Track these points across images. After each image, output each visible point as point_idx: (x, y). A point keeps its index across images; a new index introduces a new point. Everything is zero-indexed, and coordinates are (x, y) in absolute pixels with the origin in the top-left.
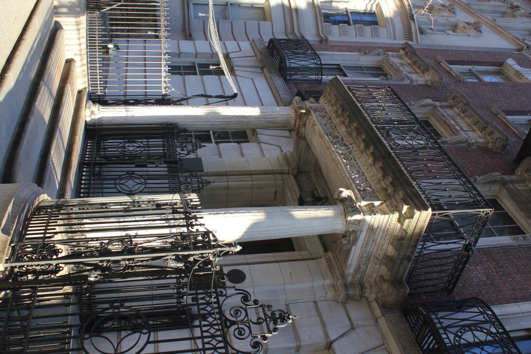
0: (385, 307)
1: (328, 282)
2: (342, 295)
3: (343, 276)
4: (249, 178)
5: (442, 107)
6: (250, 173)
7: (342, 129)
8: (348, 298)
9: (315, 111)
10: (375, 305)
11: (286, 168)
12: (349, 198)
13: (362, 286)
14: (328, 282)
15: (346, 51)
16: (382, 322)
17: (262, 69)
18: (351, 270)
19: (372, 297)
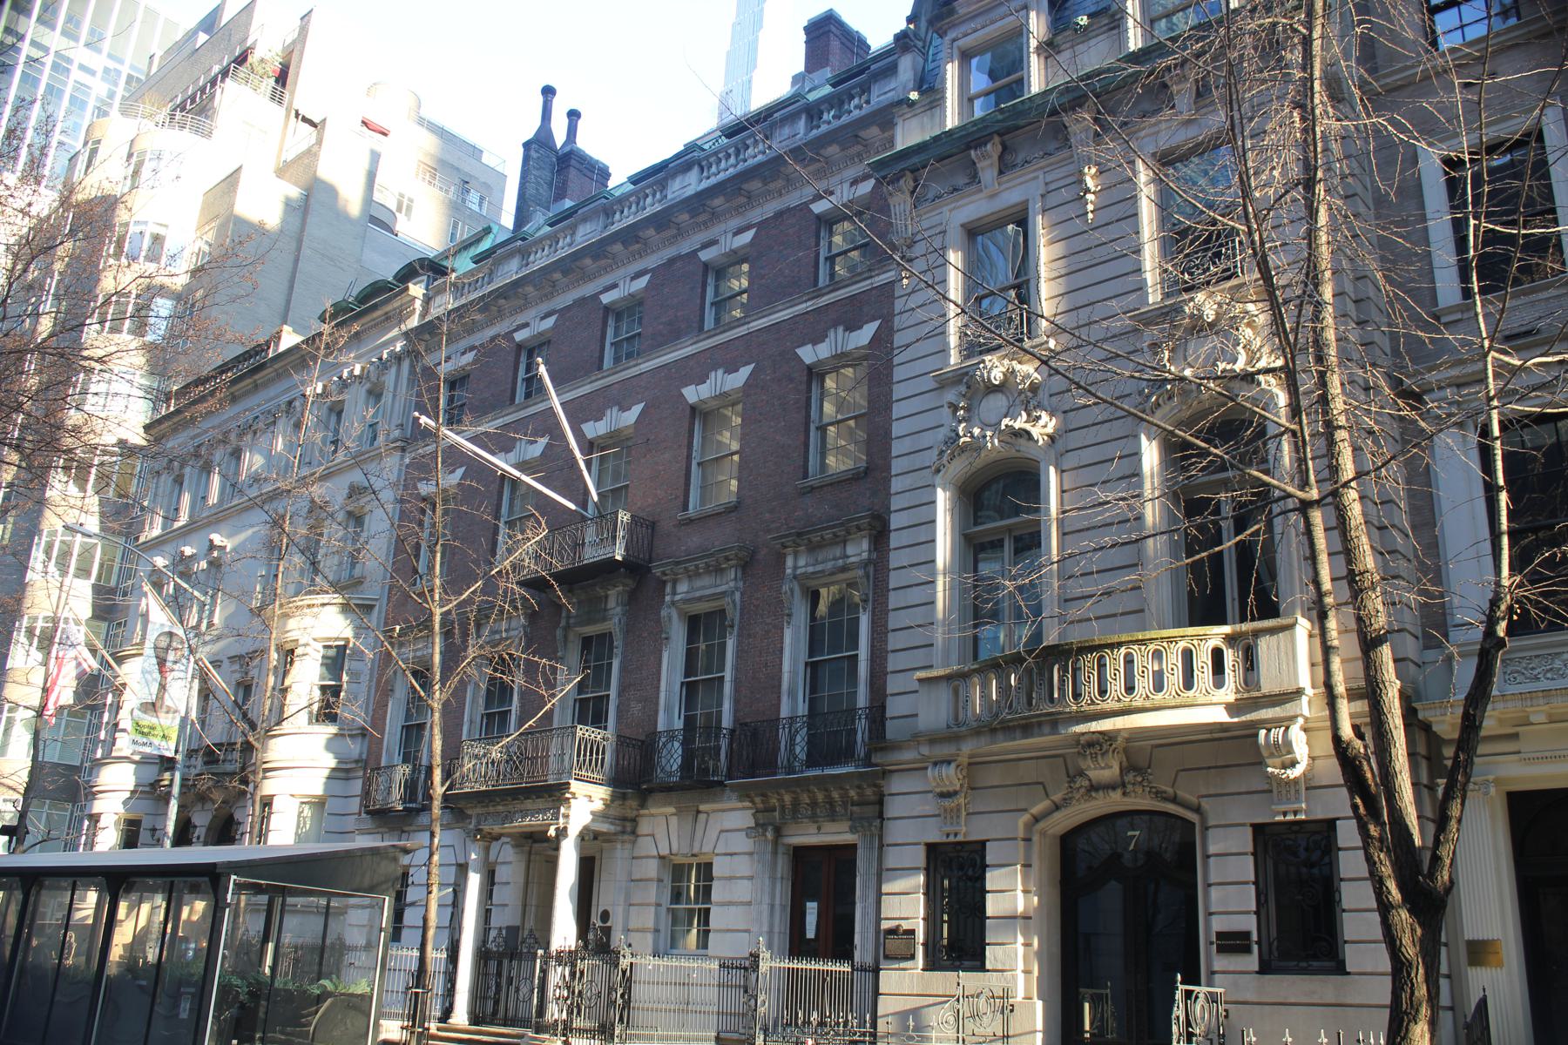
0: (643, 805)
1: (619, 846)
2: (632, 838)
3: (615, 834)
4: (530, 885)
6: (527, 883)
7: (500, 808)
8: (634, 832)
10: (642, 812)
11: (527, 849)
12: (557, 829)
13: (624, 819)
14: (619, 846)
15: (386, 712)
16: (653, 811)
17: (403, 832)
18: (612, 828)
19: (635, 813)
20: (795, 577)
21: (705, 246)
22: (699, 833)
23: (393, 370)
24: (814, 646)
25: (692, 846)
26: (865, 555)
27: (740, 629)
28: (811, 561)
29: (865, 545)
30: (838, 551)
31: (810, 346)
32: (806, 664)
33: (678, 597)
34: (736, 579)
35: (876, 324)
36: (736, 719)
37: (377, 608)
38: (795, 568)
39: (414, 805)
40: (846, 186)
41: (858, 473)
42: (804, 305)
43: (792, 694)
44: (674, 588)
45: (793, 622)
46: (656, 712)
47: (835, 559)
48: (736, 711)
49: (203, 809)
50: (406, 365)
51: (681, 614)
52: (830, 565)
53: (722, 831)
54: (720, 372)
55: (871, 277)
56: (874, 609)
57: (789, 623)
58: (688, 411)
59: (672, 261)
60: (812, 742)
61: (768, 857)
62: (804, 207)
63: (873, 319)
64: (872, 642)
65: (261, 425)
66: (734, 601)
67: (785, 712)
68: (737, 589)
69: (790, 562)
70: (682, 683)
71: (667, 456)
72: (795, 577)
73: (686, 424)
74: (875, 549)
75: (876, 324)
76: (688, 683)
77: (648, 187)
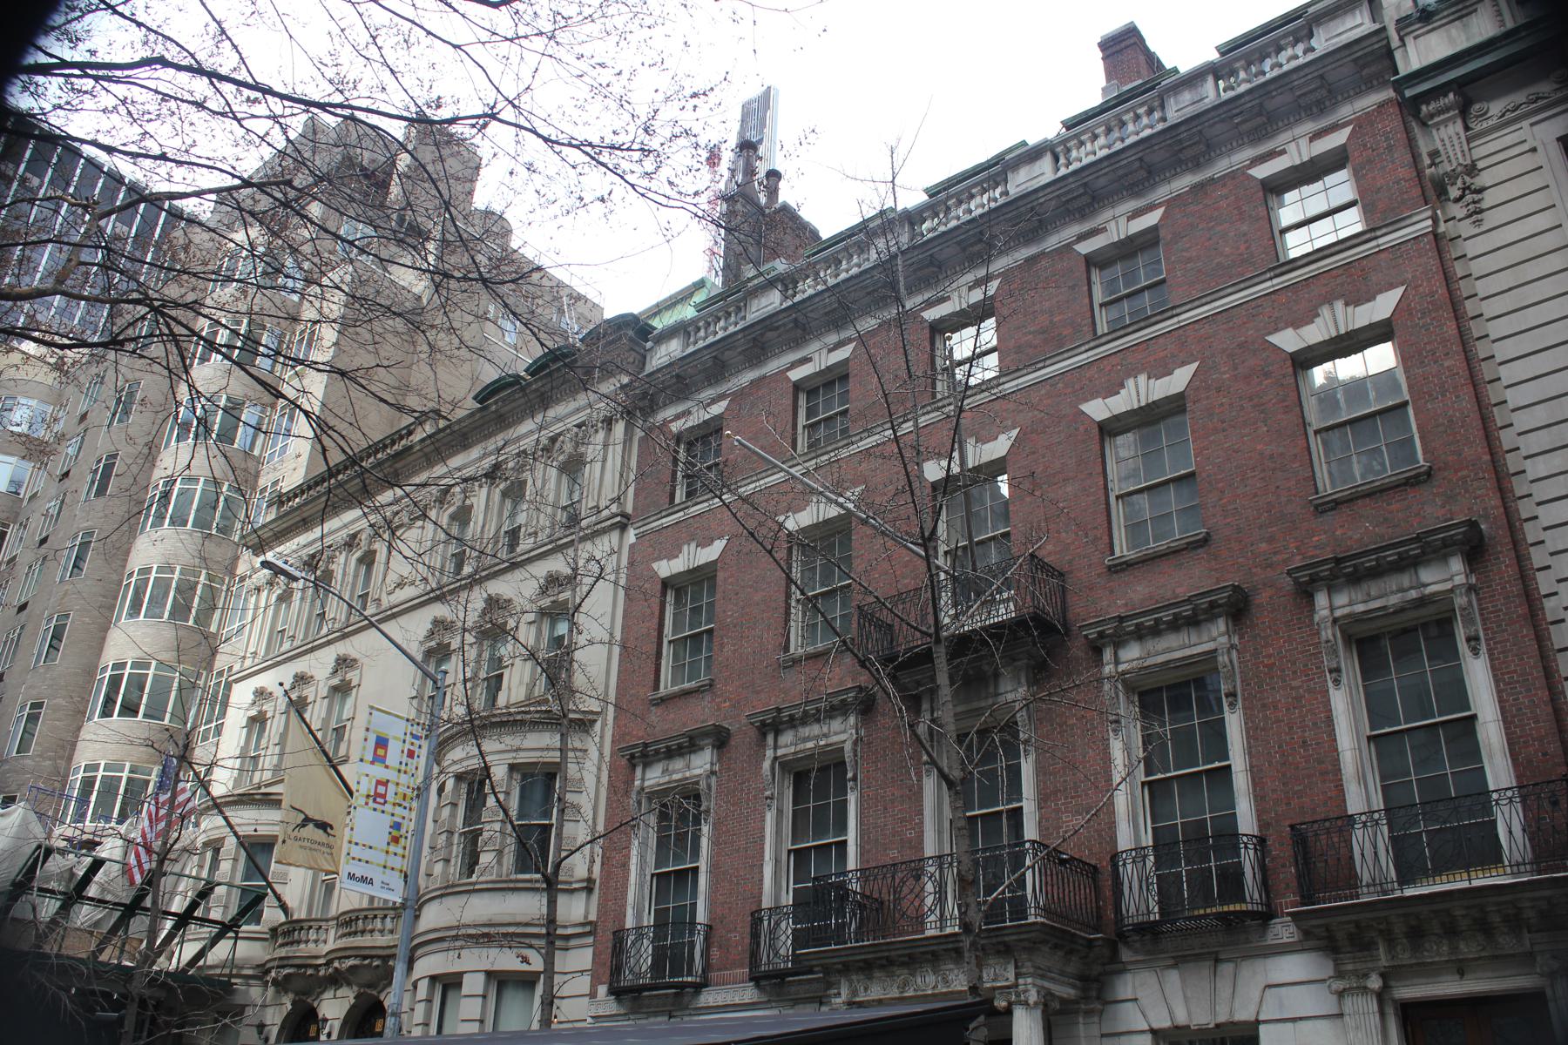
1: (1081, 1020)
3: (1076, 1002)
5: (776, 747)
9: (854, 993)
10: (1108, 968)
14: (1081, 1020)
20: (1335, 621)
21: (1082, 237)
22: (1224, 990)
23: (601, 435)
24: (1375, 717)
25: (1214, 1013)
26: (1460, 579)
27: (1244, 700)
28: (1360, 598)
29: (1457, 565)
30: (1405, 579)
31: (1290, 332)
32: (1369, 738)
33: (1121, 668)
34: (1227, 632)
35: (1399, 291)
36: (1263, 824)
37: (598, 726)
38: (1332, 609)
39: (690, 979)
40: (1303, 142)
41: (1417, 476)
42: (1269, 284)
43: (1362, 779)
44: (1116, 654)
45: (1344, 679)
46: (1112, 825)
47: (1402, 590)
48: (1260, 813)
49: (335, 997)
50: (619, 429)
51: (1130, 687)
52: (1394, 600)
53: (1270, 986)
54: (1142, 378)
55: (1376, 238)
56: (1490, 651)
57: (1337, 682)
58: (1096, 431)
59: (1031, 260)
60: (1399, 844)
61: (1375, 1019)
62: (1238, 176)
63: (1391, 287)
64: (1499, 692)
65: (406, 520)
66: (1231, 661)
67: (1355, 804)
68: (1232, 646)
69: (1321, 600)
70: (1143, 784)
71: (1069, 489)
72: (1335, 621)
73: (1096, 447)
74: (1472, 571)
75: (1399, 291)
76: (1150, 783)
77: (974, 185)
